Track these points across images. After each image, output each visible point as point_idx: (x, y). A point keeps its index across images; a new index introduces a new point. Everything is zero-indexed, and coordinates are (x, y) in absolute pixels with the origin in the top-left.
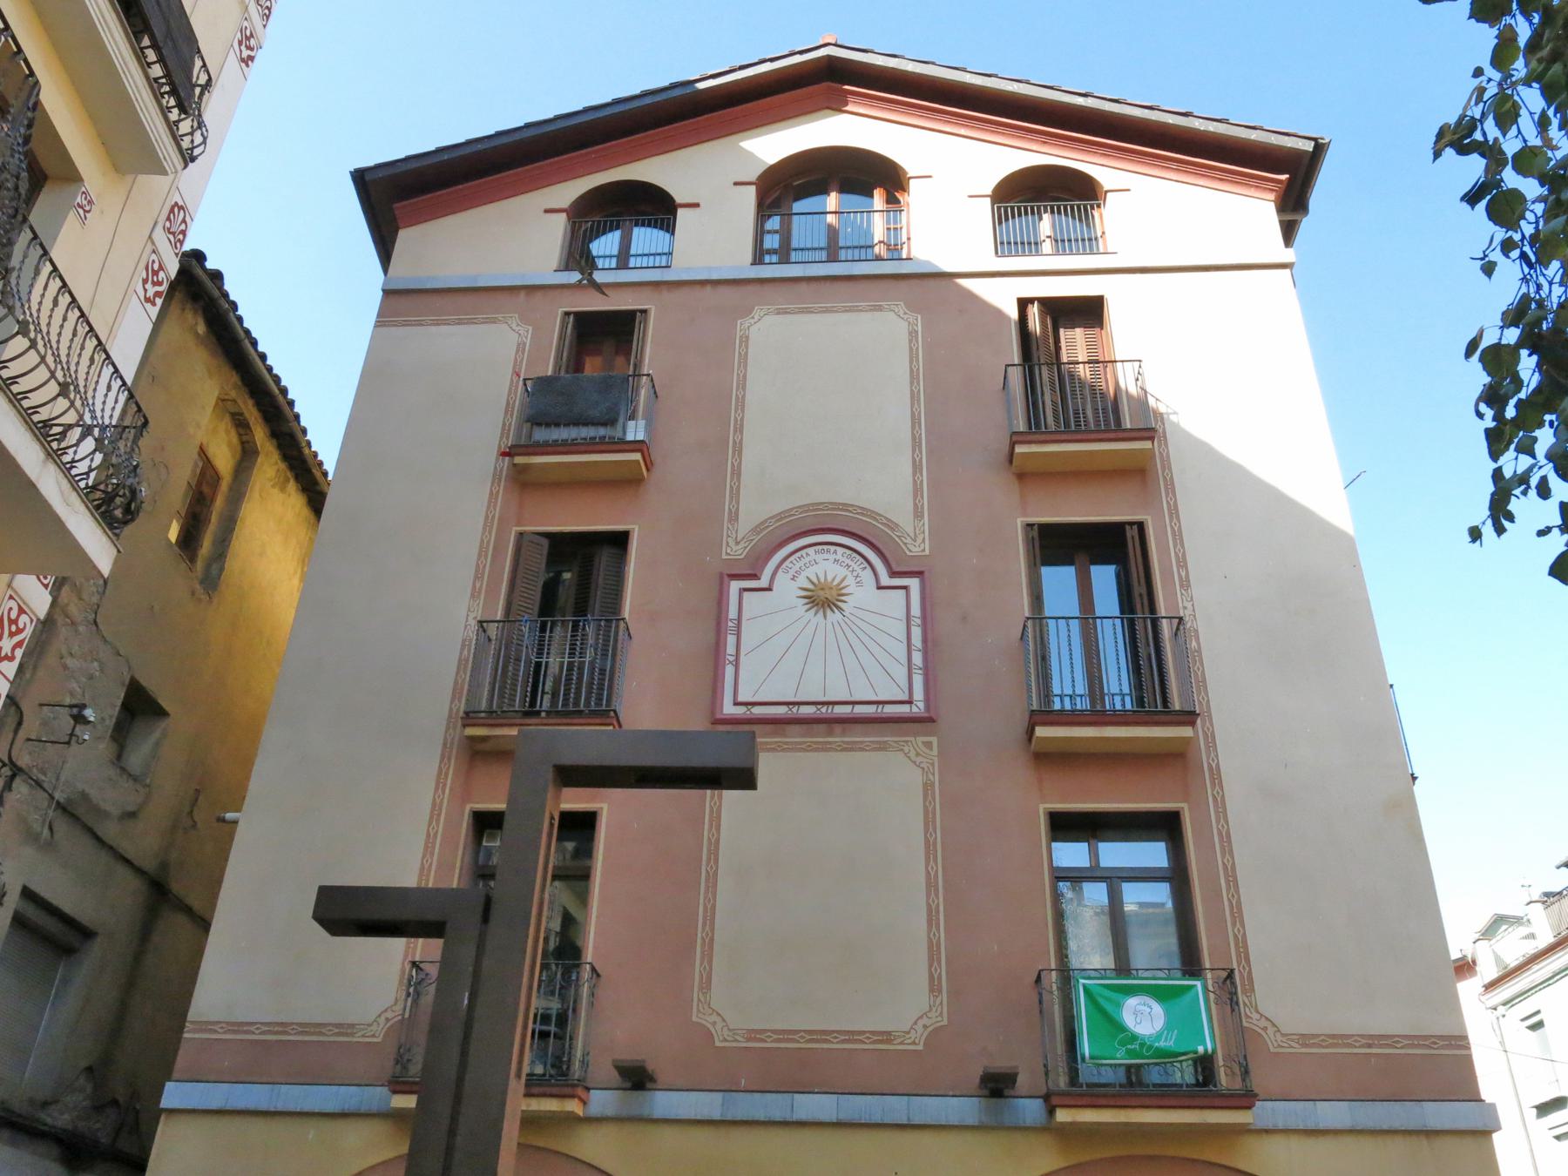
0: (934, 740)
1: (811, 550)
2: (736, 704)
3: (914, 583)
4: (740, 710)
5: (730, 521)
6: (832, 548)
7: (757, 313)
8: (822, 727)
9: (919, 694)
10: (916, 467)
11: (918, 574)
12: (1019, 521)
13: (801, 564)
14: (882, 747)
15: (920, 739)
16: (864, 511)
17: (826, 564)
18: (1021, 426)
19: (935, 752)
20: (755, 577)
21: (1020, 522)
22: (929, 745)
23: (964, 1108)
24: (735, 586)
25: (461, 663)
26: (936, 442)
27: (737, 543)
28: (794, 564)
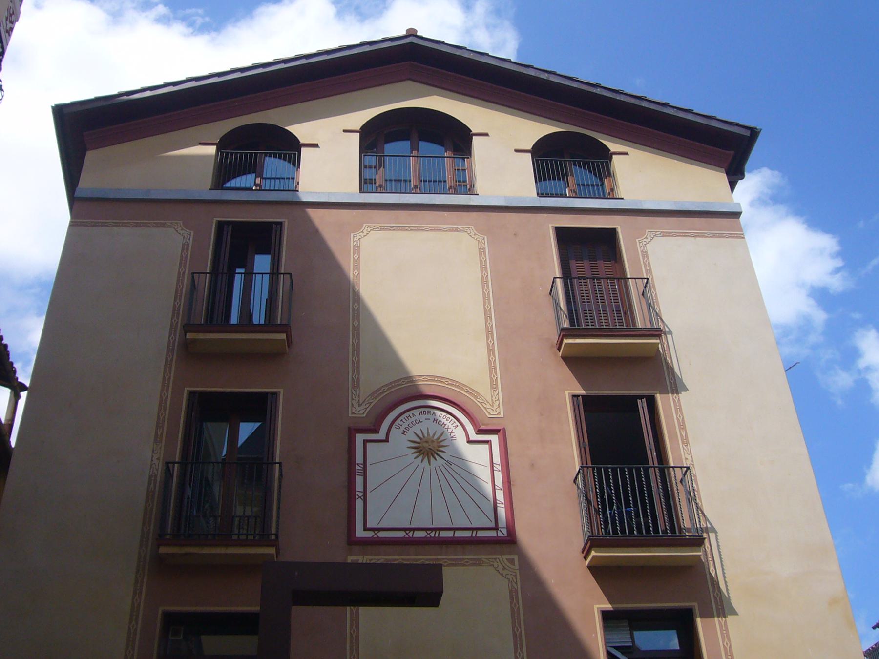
1: (416, 412)
2: (366, 529)
3: (494, 439)
4: (370, 534)
5: (353, 387)
7: (366, 228)
10: (490, 351)
12: (567, 392)
13: (409, 422)
14: (478, 563)
16: (454, 383)
18: (566, 324)
21: (567, 394)
22: (512, 561)
24: (360, 438)
26: (504, 333)
27: (360, 405)
28: (403, 422)
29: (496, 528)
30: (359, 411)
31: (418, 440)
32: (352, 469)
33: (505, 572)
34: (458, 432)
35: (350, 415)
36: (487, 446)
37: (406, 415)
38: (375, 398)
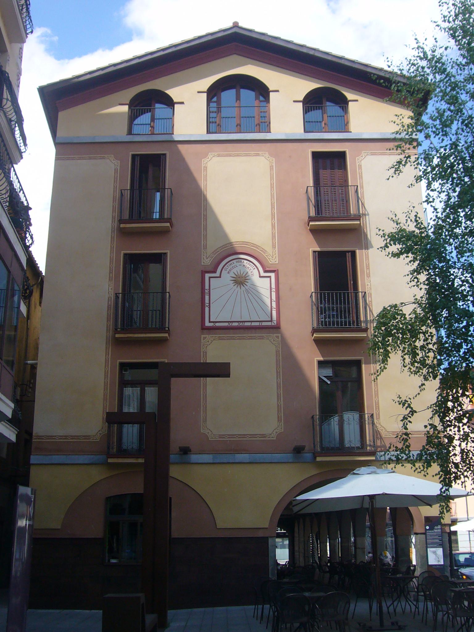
2: (210, 322)
3: (273, 275)
4: (212, 324)
7: (210, 156)
10: (273, 226)
13: (231, 267)
14: (262, 338)
15: (275, 335)
18: (313, 214)
20: (215, 272)
21: (311, 250)
22: (278, 337)
23: (289, 457)
24: (207, 276)
25: (109, 307)
26: (281, 216)
28: (228, 267)
29: (271, 321)
30: (207, 261)
31: (235, 276)
33: (274, 342)
34: (254, 272)
36: (269, 279)
37: (230, 263)
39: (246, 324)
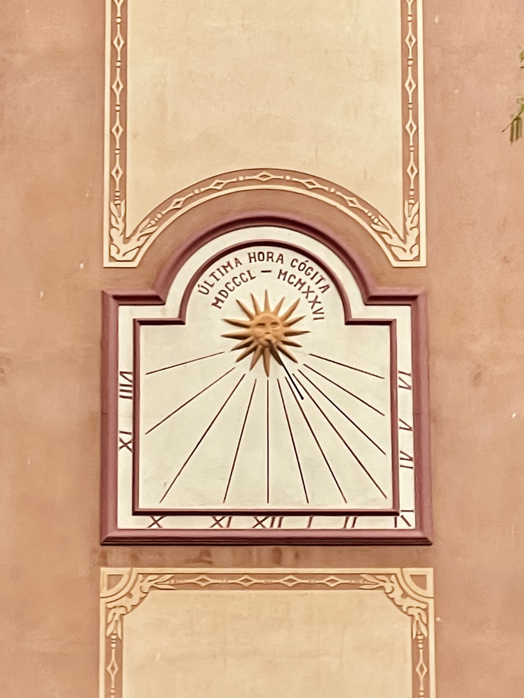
0: (429, 572)
1: (242, 254)
3: (402, 314)
5: (113, 198)
6: (277, 251)
8: (266, 550)
9: (407, 500)
11: (409, 300)
13: (228, 278)
14: (354, 584)
15: (409, 571)
17: (266, 281)
19: (430, 591)
20: (157, 300)
22: (420, 581)
24: (127, 314)
27: (126, 240)
28: (216, 280)
31: (244, 319)
32: (109, 383)
33: (406, 603)
35: (107, 263)
37: (223, 261)
38: (159, 223)
39: (290, 524)
